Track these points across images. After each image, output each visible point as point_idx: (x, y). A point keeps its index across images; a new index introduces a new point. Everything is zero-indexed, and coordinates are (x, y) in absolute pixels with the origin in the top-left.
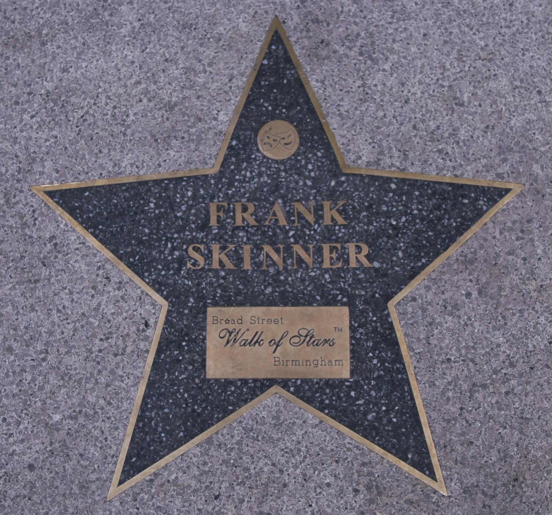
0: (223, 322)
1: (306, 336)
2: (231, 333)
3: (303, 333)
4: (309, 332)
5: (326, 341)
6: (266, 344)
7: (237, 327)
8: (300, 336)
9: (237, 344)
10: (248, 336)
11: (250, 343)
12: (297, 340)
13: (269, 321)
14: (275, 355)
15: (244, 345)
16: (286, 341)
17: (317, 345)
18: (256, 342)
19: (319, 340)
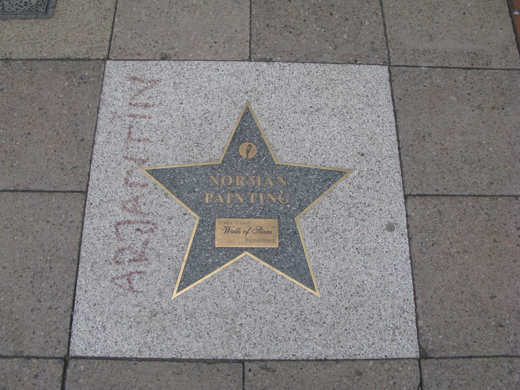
0: (224, 223)
1: (260, 229)
2: (227, 227)
3: (259, 228)
4: (261, 228)
5: (268, 232)
6: (242, 232)
7: (230, 225)
8: (256, 229)
9: (230, 232)
10: (234, 229)
11: (235, 232)
12: (255, 231)
13: (243, 223)
14: (246, 237)
15: (233, 233)
16: (250, 231)
17: (264, 233)
18: (238, 231)
19: (265, 231)
